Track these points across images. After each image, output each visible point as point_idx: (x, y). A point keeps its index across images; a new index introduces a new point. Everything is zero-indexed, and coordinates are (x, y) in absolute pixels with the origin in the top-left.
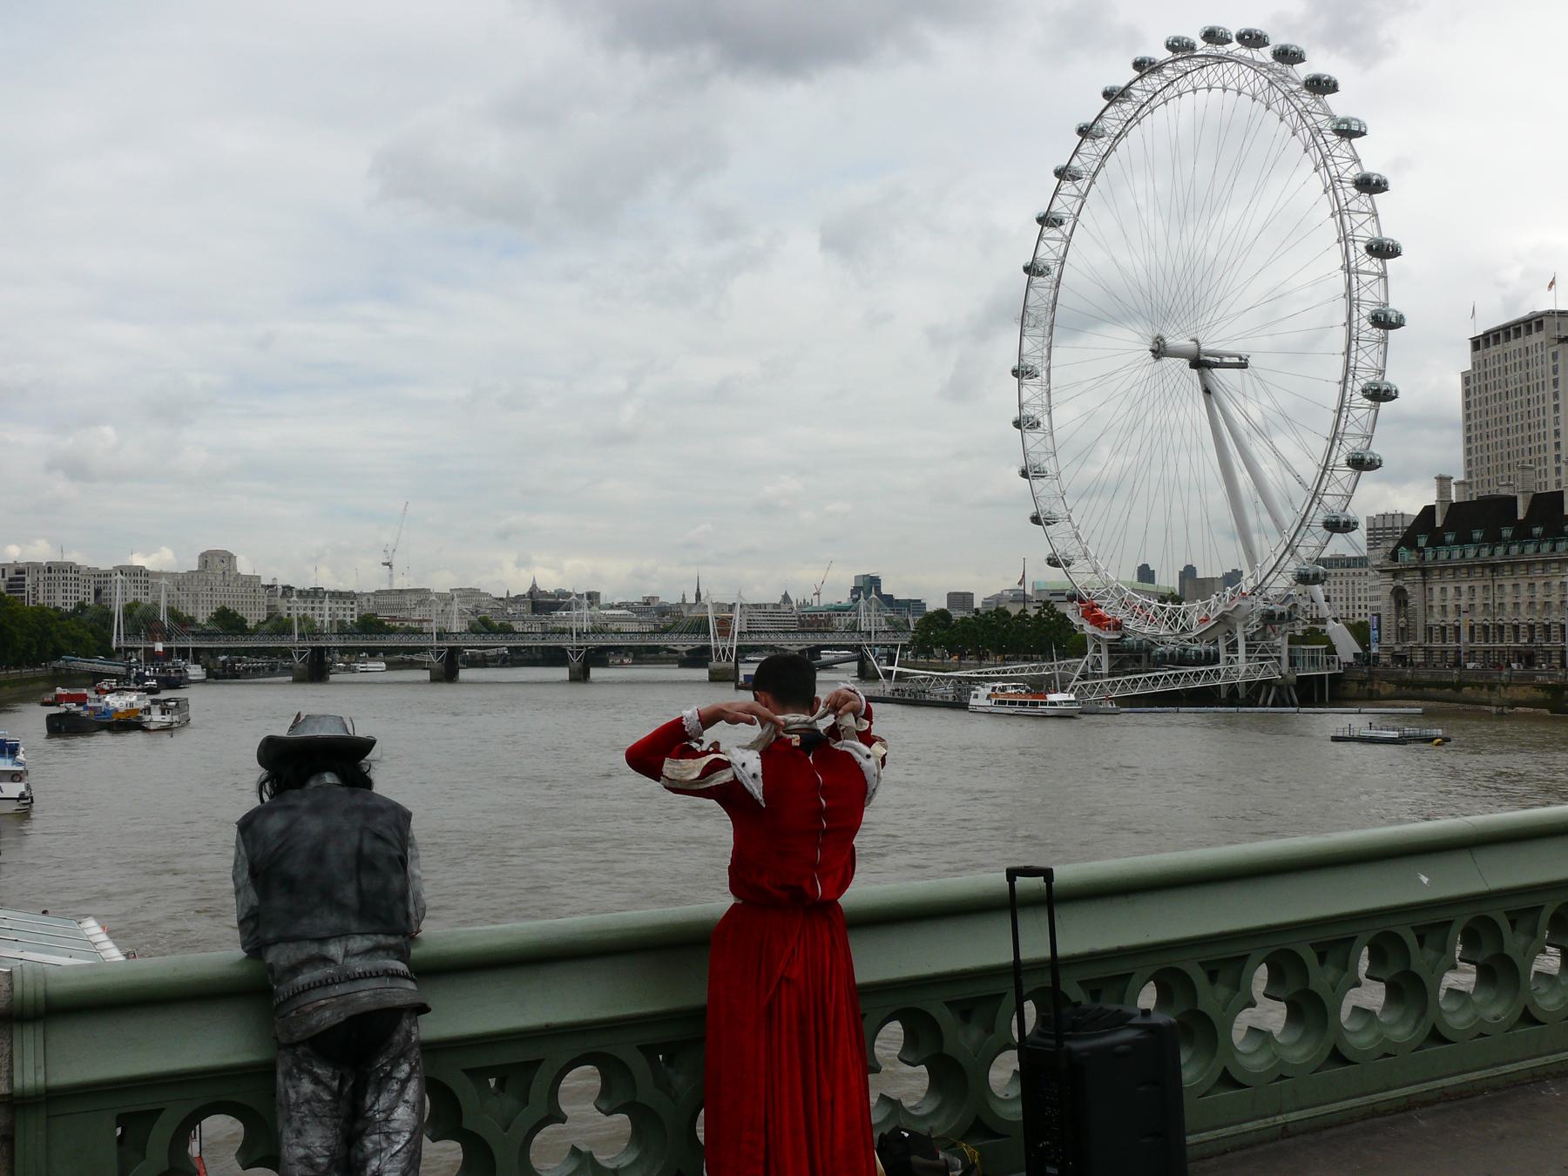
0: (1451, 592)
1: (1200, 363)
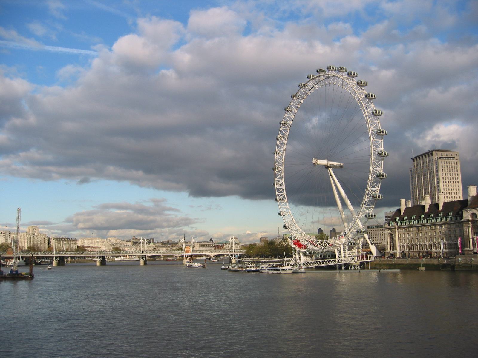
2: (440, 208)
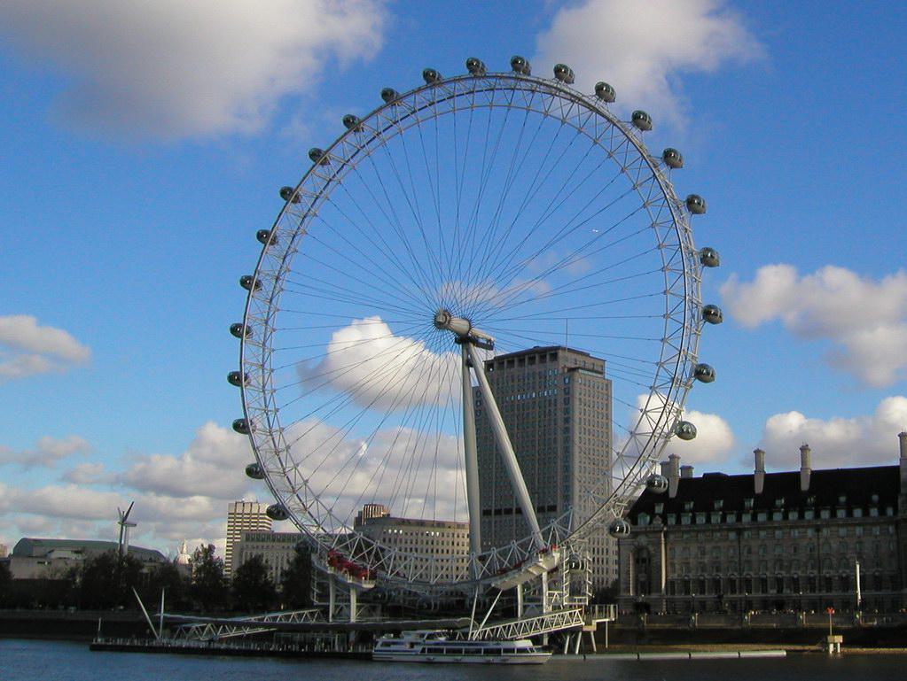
0: (694, 549)
1: (465, 340)
2: (805, 485)
